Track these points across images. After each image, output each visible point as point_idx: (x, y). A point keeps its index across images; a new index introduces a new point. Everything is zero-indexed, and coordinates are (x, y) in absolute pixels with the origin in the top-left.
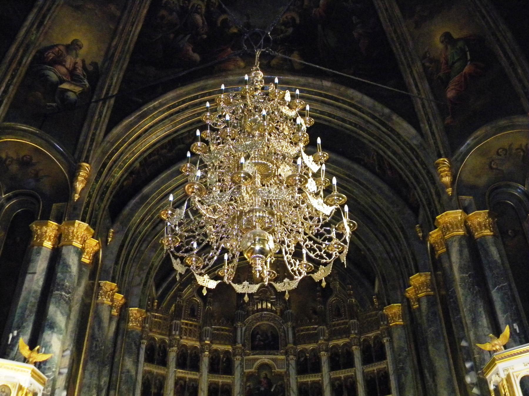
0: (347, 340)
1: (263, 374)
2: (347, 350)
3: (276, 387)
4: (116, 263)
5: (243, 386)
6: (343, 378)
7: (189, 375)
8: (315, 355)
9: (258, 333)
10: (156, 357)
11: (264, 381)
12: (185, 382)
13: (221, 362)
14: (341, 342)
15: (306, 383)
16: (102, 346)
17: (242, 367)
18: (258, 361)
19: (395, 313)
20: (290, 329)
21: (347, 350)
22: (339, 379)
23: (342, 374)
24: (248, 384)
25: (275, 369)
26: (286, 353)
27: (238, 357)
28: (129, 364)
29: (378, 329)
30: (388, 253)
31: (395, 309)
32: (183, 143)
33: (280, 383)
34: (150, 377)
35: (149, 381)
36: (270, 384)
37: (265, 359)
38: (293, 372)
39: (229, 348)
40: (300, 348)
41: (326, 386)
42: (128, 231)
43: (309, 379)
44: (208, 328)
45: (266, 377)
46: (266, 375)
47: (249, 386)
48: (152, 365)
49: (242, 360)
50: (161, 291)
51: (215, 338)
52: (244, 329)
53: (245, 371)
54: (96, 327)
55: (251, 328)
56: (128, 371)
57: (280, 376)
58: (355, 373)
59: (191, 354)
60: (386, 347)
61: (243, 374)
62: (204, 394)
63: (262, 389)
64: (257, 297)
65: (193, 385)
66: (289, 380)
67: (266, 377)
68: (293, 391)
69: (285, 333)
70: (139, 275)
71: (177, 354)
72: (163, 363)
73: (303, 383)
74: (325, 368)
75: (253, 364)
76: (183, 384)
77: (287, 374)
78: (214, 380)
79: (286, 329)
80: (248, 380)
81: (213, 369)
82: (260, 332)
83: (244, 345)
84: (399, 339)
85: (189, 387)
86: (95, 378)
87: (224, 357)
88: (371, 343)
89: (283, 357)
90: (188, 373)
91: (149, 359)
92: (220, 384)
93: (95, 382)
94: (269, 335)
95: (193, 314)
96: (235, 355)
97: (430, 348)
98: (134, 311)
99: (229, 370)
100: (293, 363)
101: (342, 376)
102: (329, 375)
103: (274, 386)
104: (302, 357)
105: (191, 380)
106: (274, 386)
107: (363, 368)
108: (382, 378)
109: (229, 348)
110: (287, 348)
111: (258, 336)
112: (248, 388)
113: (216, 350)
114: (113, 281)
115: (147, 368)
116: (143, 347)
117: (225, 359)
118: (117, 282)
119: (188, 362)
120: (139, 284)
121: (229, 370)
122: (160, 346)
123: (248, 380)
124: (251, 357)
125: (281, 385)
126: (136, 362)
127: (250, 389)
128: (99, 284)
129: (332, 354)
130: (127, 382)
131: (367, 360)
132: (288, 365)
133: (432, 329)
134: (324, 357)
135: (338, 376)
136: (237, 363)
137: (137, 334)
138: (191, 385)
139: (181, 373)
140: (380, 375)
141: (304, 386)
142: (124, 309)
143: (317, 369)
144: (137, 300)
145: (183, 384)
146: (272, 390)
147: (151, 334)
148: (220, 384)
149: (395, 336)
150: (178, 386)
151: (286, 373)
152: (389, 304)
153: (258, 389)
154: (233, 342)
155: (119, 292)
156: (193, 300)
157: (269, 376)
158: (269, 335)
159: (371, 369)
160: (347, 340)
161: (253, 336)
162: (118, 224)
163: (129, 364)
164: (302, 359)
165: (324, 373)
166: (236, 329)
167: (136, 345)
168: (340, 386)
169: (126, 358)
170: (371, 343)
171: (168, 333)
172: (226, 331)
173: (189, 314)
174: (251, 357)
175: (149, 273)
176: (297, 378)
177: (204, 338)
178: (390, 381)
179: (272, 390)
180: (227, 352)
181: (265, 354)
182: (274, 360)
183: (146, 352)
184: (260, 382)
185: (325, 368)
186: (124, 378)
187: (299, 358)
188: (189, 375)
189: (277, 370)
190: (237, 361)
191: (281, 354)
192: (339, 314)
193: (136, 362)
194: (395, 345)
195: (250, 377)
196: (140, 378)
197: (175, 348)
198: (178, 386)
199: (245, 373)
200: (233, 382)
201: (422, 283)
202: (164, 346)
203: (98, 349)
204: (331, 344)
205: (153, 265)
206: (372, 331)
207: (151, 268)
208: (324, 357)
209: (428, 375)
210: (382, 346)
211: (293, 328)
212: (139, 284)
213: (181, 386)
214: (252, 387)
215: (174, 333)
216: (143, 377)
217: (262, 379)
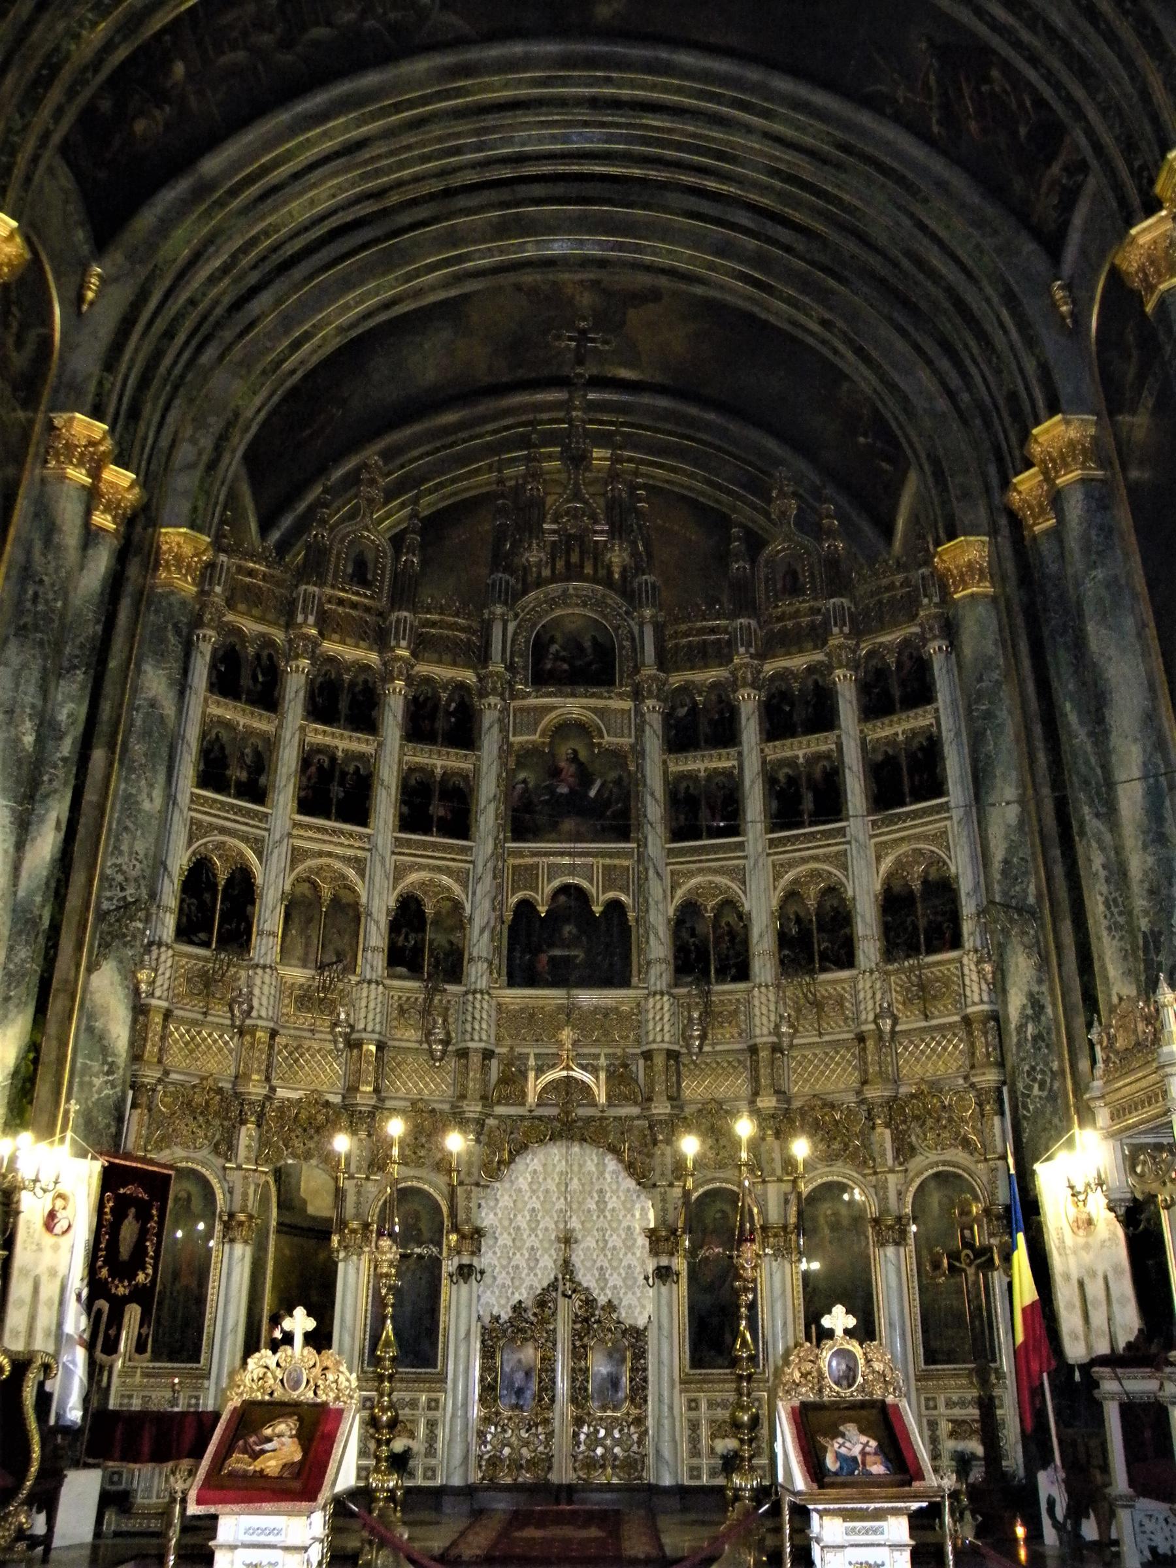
0: (819, 656)
1: (564, 750)
2: (816, 682)
3: (603, 785)
4: (110, 363)
5: (508, 783)
6: (801, 760)
7: (343, 742)
8: (720, 701)
9: (552, 640)
10: (245, 682)
11: (569, 769)
12: (333, 759)
13: (441, 714)
14: (798, 662)
15: (691, 776)
16: (55, 600)
17: (504, 730)
18: (553, 715)
19: (970, 565)
20: (649, 632)
21: (816, 682)
22: (791, 762)
23: (800, 749)
24: (522, 776)
25: (602, 737)
26: (637, 695)
27: (493, 700)
28: (155, 682)
29: (913, 617)
30: (951, 395)
31: (967, 552)
32: (329, 24)
33: (613, 775)
34: (225, 736)
35: (222, 748)
36: (585, 777)
37: (573, 706)
38: (653, 745)
39: (468, 676)
40: (676, 680)
41: (753, 782)
42: (151, 278)
43: (701, 764)
44: (406, 614)
45: (575, 759)
46: (575, 752)
47: (524, 781)
48: (231, 703)
49: (505, 710)
50: (275, 535)
51: (422, 645)
52: (511, 627)
53: (512, 739)
54: (38, 546)
55: (534, 625)
56: (153, 704)
57: (616, 756)
58: (840, 746)
59: (353, 684)
60: (936, 667)
61: (506, 750)
62: (389, 794)
63: (563, 789)
64: (555, 527)
65: (357, 768)
66: (640, 768)
67: (575, 759)
68: (652, 794)
69: (633, 639)
70: (193, 441)
71: (311, 683)
72: (268, 699)
73: (682, 777)
74: (750, 730)
75: (537, 724)
76: (326, 765)
77: (639, 752)
78: (417, 759)
79: (636, 629)
80: (520, 765)
81: (419, 729)
82: (558, 636)
83: (511, 668)
84: (980, 632)
85: (344, 774)
86: (32, 689)
87: (450, 700)
88: (891, 660)
89: (628, 705)
90: (342, 736)
91: (225, 683)
92: (438, 771)
93: (28, 699)
94: (587, 644)
95: (361, 575)
96: (483, 694)
97: (1090, 628)
98: (175, 538)
99: (464, 735)
100: (655, 721)
101: (800, 753)
102: (762, 751)
103: (598, 784)
104: (682, 706)
105: (351, 756)
106: (598, 784)
107: (862, 731)
108: (920, 755)
109: (468, 676)
110: (638, 678)
111: (554, 648)
112: (520, 786)
113: (428, 680)
114: (97, 413)
115: (214, 711)
116: (206, 649)
117: (453, 705)
118: (109, 418)
119: (343, 705)
120: (191, 466)
121: (464, 735)
122: (258, 656)
123: (520, 765)
124: (532, 701)
125: (619, 782)
126: (182, 688)
127: (526, 790)
128: (50, 421)
129: (771, 697)
130: (146, 734)
131: (876, 705)
132: (640, 730)
133: (1100, 574)
134: (748, 703)
135: (789, 754)
136: (489, 718)
137: (184, 603)
138: (351, 769)
139: (322, 735)
140: (915, 744)
141: (683, 785)
142: (138, 527)
143: (725, 733)
144: (185, 507)
145: (326, 765)
146: (592, 793)
147: (230, 617)
148: (438, 771)
149: (970, 628)
150: (313, 769)
151: (633, 747)
152: (952, 536)
153: (551, 790)
154: (479, 656)
155: (122, 460)
156: (362, 536)
157: (583, 755)
158: (587, 644)
159: (887, 732)
160: (819, 656)
161: (540, 647)
162: (117, 256)
163: (155, 682)
164: (682, 712)
165: (745, 748)
166: (487, 627)
167: (178, 631)
168: (792, 781)
169: (147, 667)
170: (891, 660)
171: (282, 621)
172: (463, 629)
173: (352, 576)
174: (532, 701)
175: (222, 439)
176: (664, 762)
177: (393, 643)
178: (943, 759)
179: (592, 793)
180: (461, 687)
181: (573, 695)
182: (600, 712)
183: (213, 666)
184: (555, 772)
185: (750, 730)
186: (138, 723)
187: (673, 708)
188: (343, 742)
189: (608, 740)
190: (490, 710)
191: (621, 696)
192: (794, 588)
193: (182, 688)
194: (968, 651)
195: (526, 756)
196: (192, 733)
197: (305, 663)
198: (313, 769)
199: (511, 745)
200: (477, 770)
201: (1071, 444)
202: (270, 656)
203: (40, 608)
204: (770, 668)
205: (237, 415)
206: (895, 625)
207: (230, 424)
208: (748, 703)
209: (1073, 718)
210: (923, 667)
211: (659, 629)
212: (191, 466)
213: (320, 768)
214: (531, 785)
215: (300, 618)
216: (204, 735)
217: (563, 764)
